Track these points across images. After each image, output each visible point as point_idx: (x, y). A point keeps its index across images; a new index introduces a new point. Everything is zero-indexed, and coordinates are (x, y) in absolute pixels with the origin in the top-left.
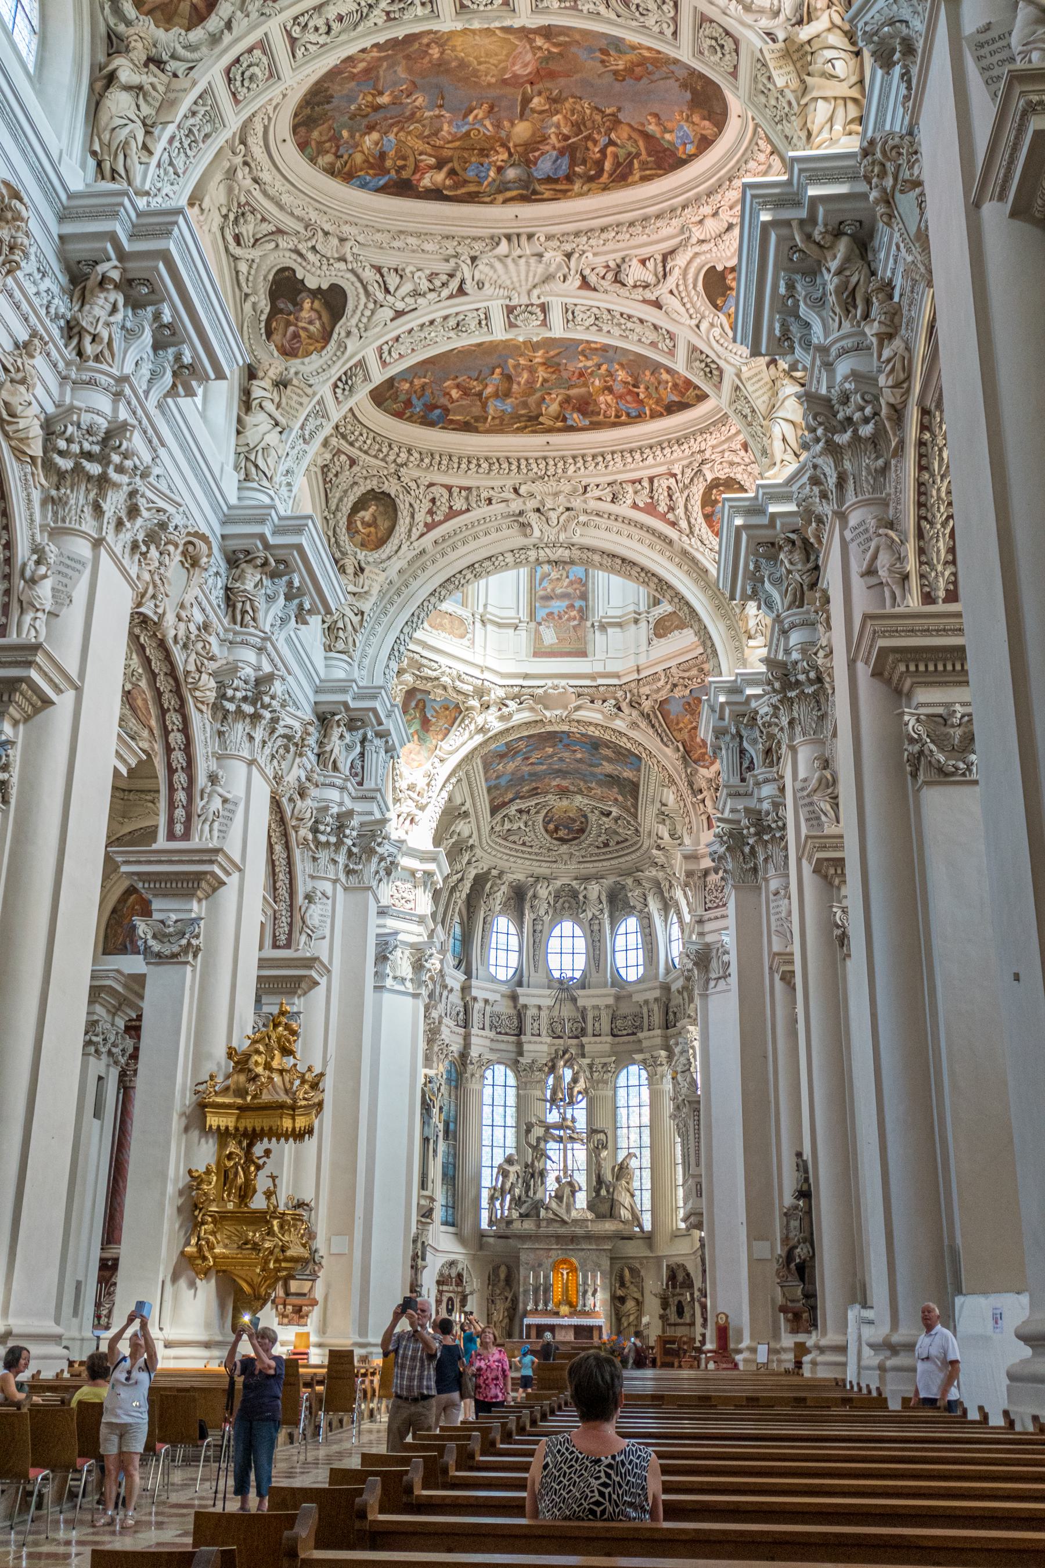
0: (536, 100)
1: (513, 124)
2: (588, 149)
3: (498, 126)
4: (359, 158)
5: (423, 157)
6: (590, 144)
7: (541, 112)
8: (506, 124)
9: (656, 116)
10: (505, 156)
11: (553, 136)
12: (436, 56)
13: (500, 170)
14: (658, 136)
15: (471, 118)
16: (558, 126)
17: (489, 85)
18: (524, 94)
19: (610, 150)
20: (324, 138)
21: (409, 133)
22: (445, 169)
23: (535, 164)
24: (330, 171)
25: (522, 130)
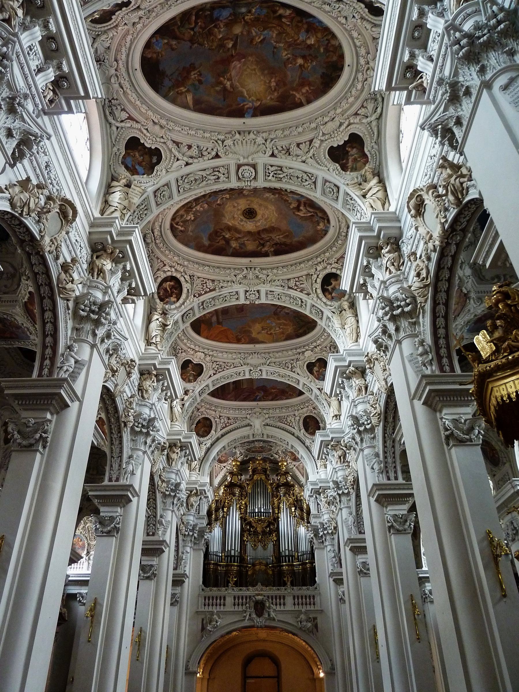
0: (230, 45)
1: (242, 32)
2: (204, 23)
3: (249, 32)
4: (319, 35)
5: (288, 23)
6: (203, 25)
7: (228, 39)
8: (245, 33)
9: (173, 49)
10: (246, 18)
11: (222, 26)
12: (273, 80)
13: (250, 12)
14: (170, 40)
15: (262, 38)
16: (220, 32)
17: (251, 55)
18: (236, 49)
19: (193, 26)
20: (331, 53)
21: (292, 37)
22: (278, 14)
23: (231, 14)
24: (334, 36)
25: (237, 30)
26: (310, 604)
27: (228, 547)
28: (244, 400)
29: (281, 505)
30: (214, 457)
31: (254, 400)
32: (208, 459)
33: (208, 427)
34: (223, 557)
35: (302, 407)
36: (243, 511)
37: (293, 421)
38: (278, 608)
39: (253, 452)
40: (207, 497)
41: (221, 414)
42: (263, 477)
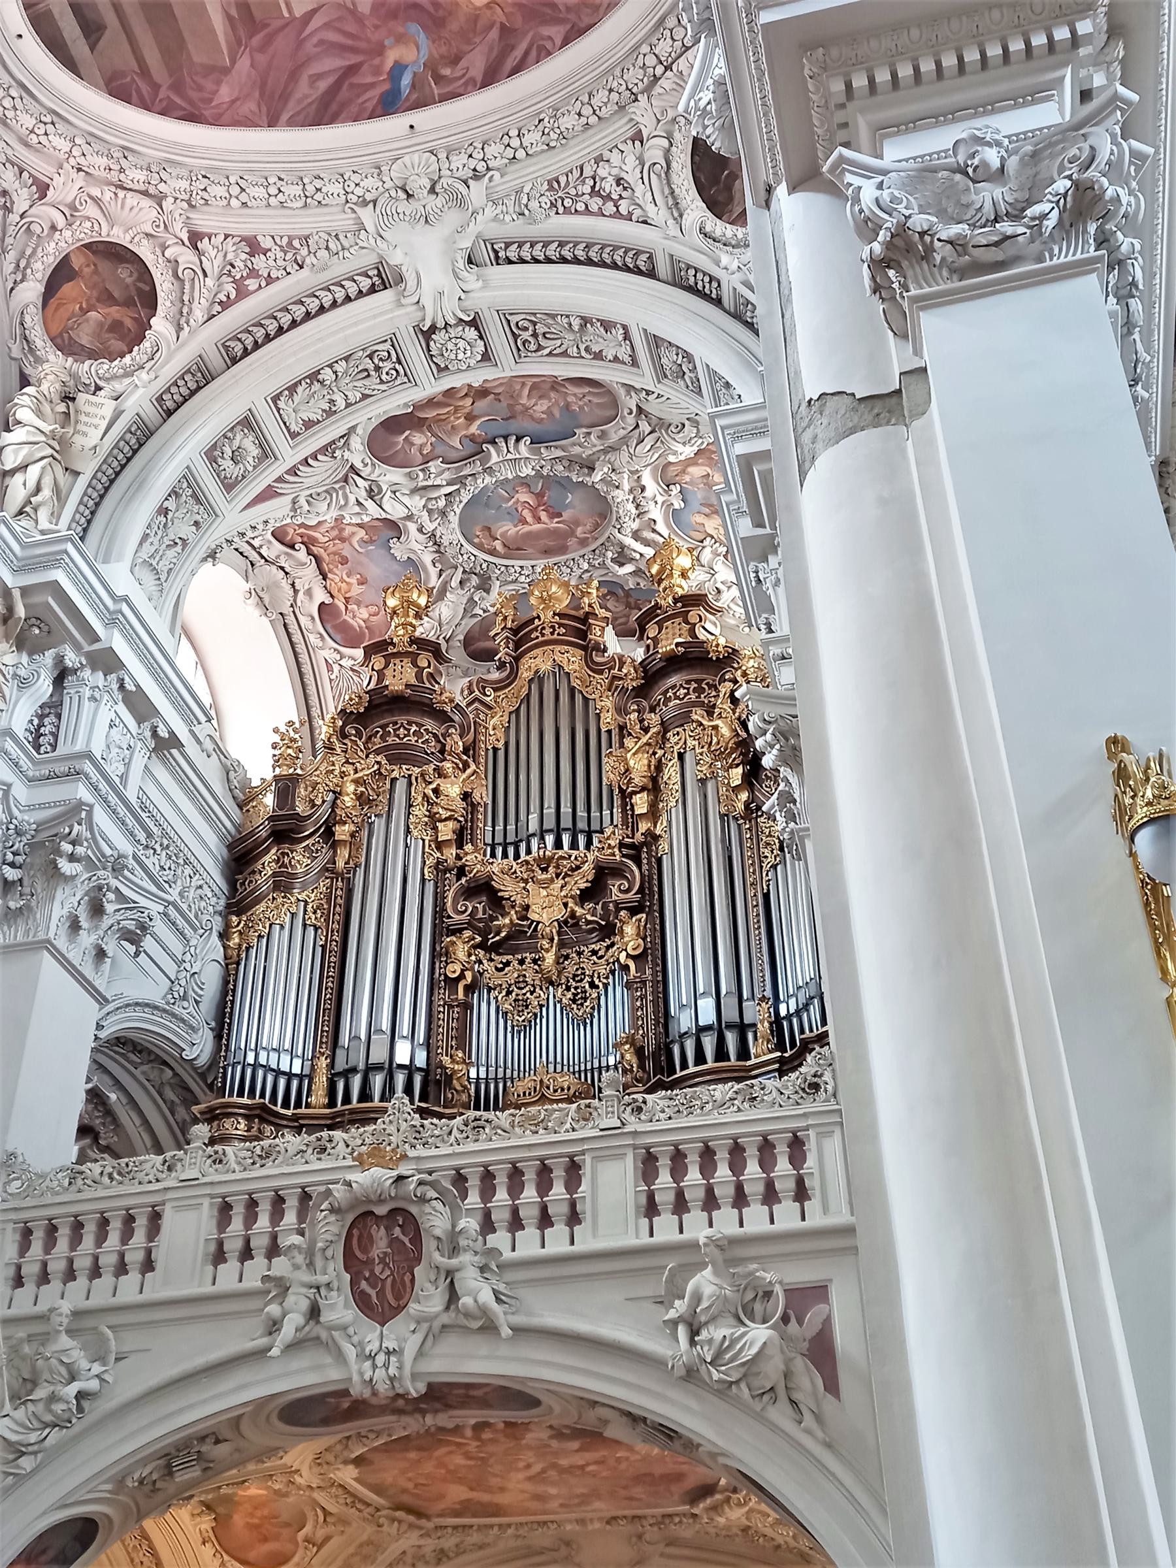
26: (770, 1196)
27: (356, 1022)
28: (324, 113)
29: (671, 772)
30: (188, 477)
31: (389, 105)
32: (140, 484)
33: (128, 303)
34: (321, 1080)
35: (664, 48)
36: (446, 831)
37: (632, 178)
38: (528, 1244)
39: (514, 549)
40: (107, 662)
41: (202, 222)
42: (572, 660)
